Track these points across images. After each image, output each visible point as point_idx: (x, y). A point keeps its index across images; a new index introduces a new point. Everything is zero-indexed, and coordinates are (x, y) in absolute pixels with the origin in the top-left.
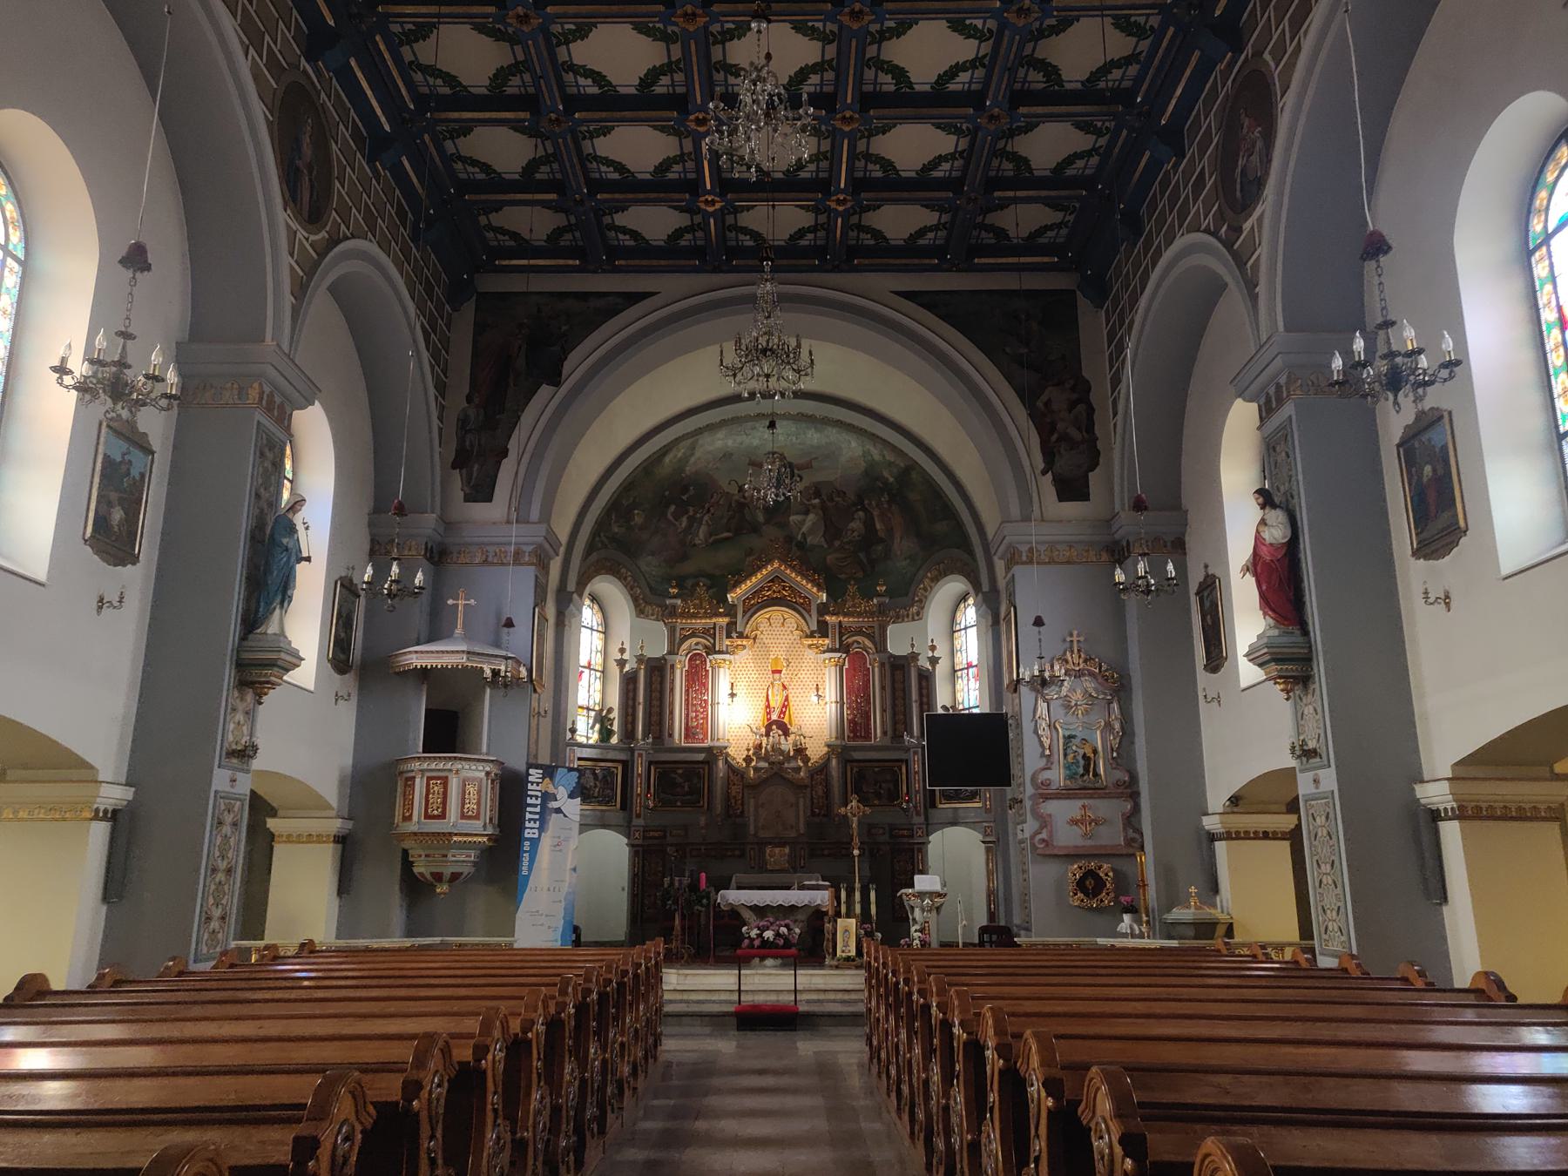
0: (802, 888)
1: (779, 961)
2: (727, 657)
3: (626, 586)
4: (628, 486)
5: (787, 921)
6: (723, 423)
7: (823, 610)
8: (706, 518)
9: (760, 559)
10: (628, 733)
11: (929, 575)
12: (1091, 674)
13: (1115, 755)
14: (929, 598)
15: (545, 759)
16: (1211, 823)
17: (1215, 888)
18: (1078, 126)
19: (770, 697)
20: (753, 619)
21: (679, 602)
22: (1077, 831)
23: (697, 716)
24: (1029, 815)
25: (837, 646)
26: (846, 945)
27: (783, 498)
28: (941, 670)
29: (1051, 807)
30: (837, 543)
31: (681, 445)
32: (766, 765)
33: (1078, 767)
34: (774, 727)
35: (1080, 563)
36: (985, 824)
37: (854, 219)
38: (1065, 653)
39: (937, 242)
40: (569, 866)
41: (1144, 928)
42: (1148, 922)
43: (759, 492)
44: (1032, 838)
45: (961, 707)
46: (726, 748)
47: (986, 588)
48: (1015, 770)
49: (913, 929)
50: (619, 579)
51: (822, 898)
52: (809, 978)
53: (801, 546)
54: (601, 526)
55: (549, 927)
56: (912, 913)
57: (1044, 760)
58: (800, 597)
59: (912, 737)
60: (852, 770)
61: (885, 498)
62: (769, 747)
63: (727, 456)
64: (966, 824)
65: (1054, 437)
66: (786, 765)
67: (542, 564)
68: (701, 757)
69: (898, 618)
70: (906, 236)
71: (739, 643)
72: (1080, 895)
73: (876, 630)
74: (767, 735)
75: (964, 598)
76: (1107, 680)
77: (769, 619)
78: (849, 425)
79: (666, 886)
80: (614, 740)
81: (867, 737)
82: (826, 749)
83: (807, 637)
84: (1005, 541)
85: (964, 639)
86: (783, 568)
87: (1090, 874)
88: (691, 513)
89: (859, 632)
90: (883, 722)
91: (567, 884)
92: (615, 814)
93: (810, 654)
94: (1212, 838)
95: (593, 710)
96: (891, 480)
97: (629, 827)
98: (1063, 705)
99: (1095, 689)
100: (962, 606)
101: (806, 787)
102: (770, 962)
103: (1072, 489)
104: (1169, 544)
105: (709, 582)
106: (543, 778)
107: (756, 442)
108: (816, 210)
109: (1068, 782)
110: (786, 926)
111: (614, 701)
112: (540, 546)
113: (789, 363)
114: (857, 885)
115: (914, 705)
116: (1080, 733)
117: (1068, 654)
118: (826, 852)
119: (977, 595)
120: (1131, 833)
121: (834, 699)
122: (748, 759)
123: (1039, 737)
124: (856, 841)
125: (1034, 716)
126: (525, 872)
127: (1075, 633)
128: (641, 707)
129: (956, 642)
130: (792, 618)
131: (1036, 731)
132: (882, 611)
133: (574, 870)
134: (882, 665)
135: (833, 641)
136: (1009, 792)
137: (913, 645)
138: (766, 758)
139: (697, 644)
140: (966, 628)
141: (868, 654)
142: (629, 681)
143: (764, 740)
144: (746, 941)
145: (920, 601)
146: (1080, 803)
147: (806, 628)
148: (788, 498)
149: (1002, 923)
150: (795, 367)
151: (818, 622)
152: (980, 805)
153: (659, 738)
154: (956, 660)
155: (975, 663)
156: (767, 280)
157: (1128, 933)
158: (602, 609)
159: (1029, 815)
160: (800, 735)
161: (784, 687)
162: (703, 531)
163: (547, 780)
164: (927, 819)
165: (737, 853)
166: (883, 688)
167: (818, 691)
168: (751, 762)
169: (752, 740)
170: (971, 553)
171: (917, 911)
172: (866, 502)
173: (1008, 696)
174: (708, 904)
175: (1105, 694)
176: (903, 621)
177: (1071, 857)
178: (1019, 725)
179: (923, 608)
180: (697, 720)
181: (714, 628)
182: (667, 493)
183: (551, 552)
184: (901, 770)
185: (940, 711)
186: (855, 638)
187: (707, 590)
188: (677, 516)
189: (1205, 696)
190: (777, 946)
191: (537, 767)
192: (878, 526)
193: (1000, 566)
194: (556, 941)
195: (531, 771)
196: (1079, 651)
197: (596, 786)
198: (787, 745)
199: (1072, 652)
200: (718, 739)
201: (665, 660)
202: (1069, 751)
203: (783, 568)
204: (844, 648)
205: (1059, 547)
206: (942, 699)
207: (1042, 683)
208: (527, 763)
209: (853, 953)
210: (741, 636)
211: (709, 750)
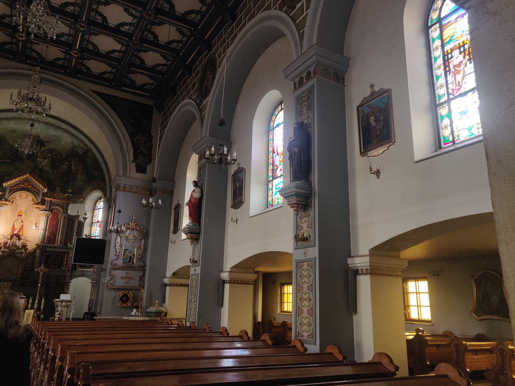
6: (14, 118)
7: (45, 195)
9: (21, 173)
11: (89, 188)
12: (137, 230)
13: (140, 257)
14: (88, 197)
16: (166, 281)
17: (164, 301)
18: (162, 56)
19: (15, 225)
20: (13, 194)
22: (123, 281)
24: (108, 275)
25: (48, 209)
28: (87, 223)
29: (116, 273)
30: (55, 172)
32: (8, 250)
34: (14, 236)
35: (140, 193)
36: (93, 277)
37: (80, 61)
38: (129, 222)
39: (110, 78)
41: (140, 314)
42: (141, 312)
43: (21, 149)
44: (107, 283)
45: (92, 236)
47: (108, 196)
49: (56, 314)
53: (41, 170)
56: (57, 308)
58: (36, 189)
59: (71, 245)
60: (45, 254)
61: (77, 159)
62: (11, 244)
63: (14, 131)
64: (85, 276)
65: (138, 151)
69: (74, 202)
71: (5, 203)
72: (120, 302)
73: (65, 206)
74: (11, 239)
75: (100, 198)
76: (141, 232)
77: (20, 195)
78: (67, 131)
81: (54, 243)
82: (36, 246)
83: (36, 204)
84: (116, 182)
85: (98, 212)
86: (30, 177)
87: (125, 295)
89: (58, 205)
93: (36, 211)
94: (166, 285)
96: (81, 153)
98: (126, 239)
99: (137, 235)
100: (99, 201)
101: (24, 260)
103: (141, 169)
104: (168, 192)
108: (65, 53)
109: (123, 264)
118: (28, 284)
120: (141, 283)
121: (43, 228)
123: (116, 249)
124: (40, 281)
125: (115, 242)
127: (134, 216)
129: (95, 213)
130: (30, 197)
131: (115, 247)
132: (68, 198)
134: (65, 218)
136: (104, 266)
138: (8, 248)
140: (99, 209)
141: (60, 213)
143: (9, 241)
145: (84, 197)
146: (126, 271)
147: (36, 201)
148: (34, 153)
151: (42, 199)
152: (93, 270)
154: (94, 219)
155: (100, 221)
157: (135, 315)
159: (108, 275)
160: (25, 240)
161: (22, 222)
164: (72, 273)
166: (63, 226)
167: (36, 224)
170: (105, 184)
171: (59, 307)
172: (70, 159)
175: (140, 237)
176: (76, 203)
177: (119, 289)
178: (110, 244)
179: (84, 200)
184: (65, 256)
185: (84, 237)
189: (171, 241)
193: (113, 190)
196: (134, 222)
198: (19, 243)
199: (132, 222)
202: (125, 254)
203: (30, 177)
204: (51, 210)
206: (86, 232)
207: (117, 232)
210: (6, 200)
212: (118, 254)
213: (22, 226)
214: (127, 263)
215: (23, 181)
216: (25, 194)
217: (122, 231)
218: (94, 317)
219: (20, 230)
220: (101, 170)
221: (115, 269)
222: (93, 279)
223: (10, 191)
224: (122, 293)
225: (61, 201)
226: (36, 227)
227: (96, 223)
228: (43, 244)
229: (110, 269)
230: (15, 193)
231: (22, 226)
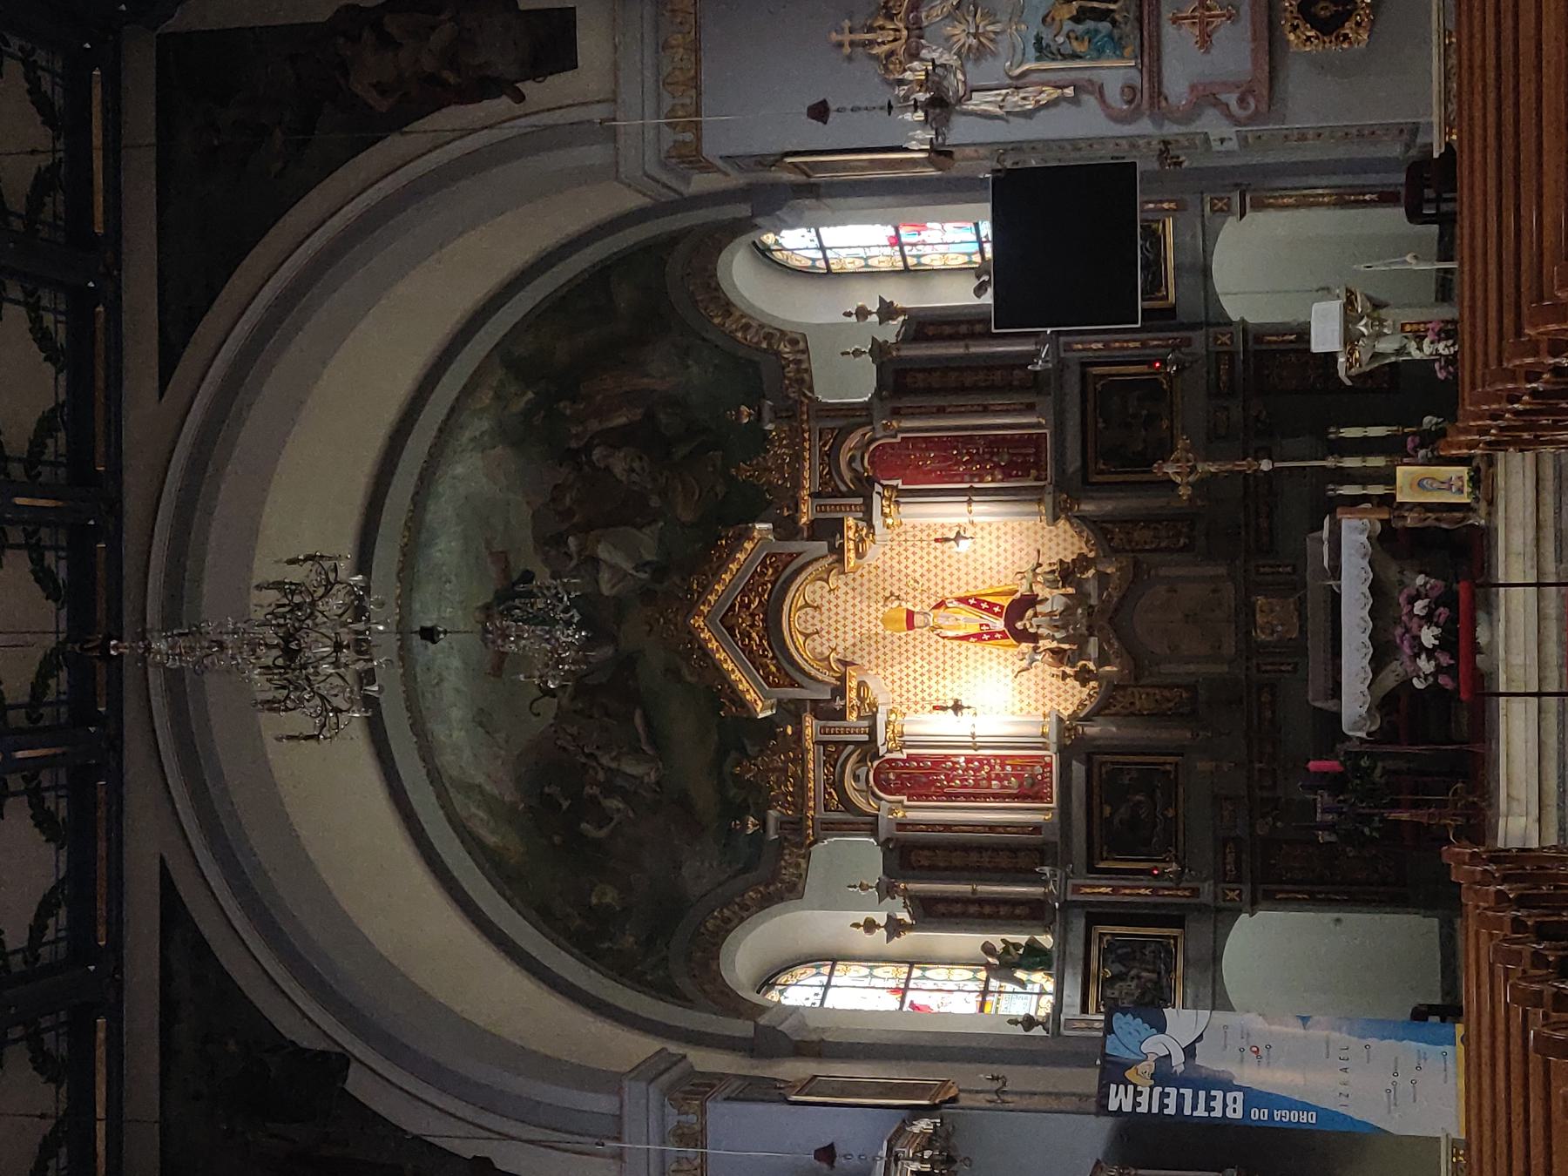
0: (1336, 571)
1: (1481, 616)
3: (742, 920)
4: (544, 916)
5: (1402, 600)
6: (419, 728)
7: (787, 529)
8: (605, 761)
10: (1033, 913)
11: (716, 321)
14: (764, 321)
15: (1087, 1079)
19: (961, 633)
20: (807, 667)
21: (772, 813)
22: (1224, 33)
23: (998, 777)
24: (1192, 128)
25: (860, 501)
26: (1447, 485)
27: (574, 612)
28: (905, 297)
29: (1177, 86)
30: (655, 502)
31: (464, 814)
32: (1093, 641)
33: (1097, 31)
34: (1019, 625)
35: (698, 26)
36: (1208, 208)
39: (62, 307)
40: (1300, 1031)
44: (1237, 122)
45: (977, 258)
46: (1060, 720)
47: (744, 210)
48: (1103, 155)
49: (1416, 355)
50: (729, 931)
51: (1355, 533)
52: (1513, 558)
53: (660, 571)
54: (623, 970)
55: (1418, 1068)
56: (1383, 355)
57: (1085, 97)
58: (763, 574)
59: (1037, 354)
61: (566, 407)
62: (1058, 635)
63: (483, 720)
64: (1207, 253)
66: (1093, 601)
67: (702, 1087)
69: (803, 380)
70: (49, 368)
71: (853, 694)
73: (831, 424)
74: (1035, 638)
75: (763, 252)
77: (807, 636)
78: (421, 478)
79: (1333, 838)
80: (1047, 940)
82: (1061, 523)
83: (841, 560)
85: (843, 253)
86: (705, 609)
88: (596, 790)
89: (831, 457)
90: (1007, 412)
91: (1335, 1035)
92: (1196, 934)
93: (874, 552)
95: (987, 982)
96: (530, 395)
97: (1219, 910)
100: (778, 255)
101: (1136, 564)
102: (1482, 636)
105: (734, 755)
106: (1126, 1083)
107: (456, 663)
109: (1127, 52)
110: (1412, 601)
111: (969, 941)
112: (668, 1092)
113: (313, 604)
114: (1330, 463)
116: (1031, 28)
117: (876, 50)
118: (1264, 524)
119: (756, 227)
121: (964, 508)
122: (1083, 677)
123: (1039, 108)
124: (1243, 465)
126: (1312, 1118)
128: (981, 888)
129: (850, 267)
130: (807, 590)
131: (1028, 115)
132: (789, 413)
133: (1305, 1020)
134: (896, 413)
136: (1146, 164)
137: (857, 353)
138: (1081, 642)
139: (856, 778)
140: (822, 248)
142: (931, 913)
144: (1443, 680)
145: (768, 337)
146: (1168, 30)
147: (825, 563)
149: (1402, 178)
150: (321, 591)
151: (811, 538)
152: (1170, 223)
153: (1042, 853)
154: (885, 267)
155: (890, 231)
156: (148, 649)
158: (788, 966)
159: (1192, 128)
160: (1035, 575)
162: (631, 768)
163: (1129, 1074)
164: (1194, 326)
165: (1265, 698)
166: (941, 411)
167: (947, 540)
168: (1090, 671)
169: (1044, 669)
170: (673, 240)
171: (1385, 346)
172: (574, 445)
173: (959, 168)
174: (1370, 755)
176: (808, 371)
178: (1017, 147)
179: (782, 333)
180: (1007, 777)
181: (825, 744)
182: (557, 839)
183: (675, 1072)
185: (988, 298)
187: (749, 758)
188: (603, 819)
190: (1453, 620)
191: (1103, 1096)
193: (701, 183)
194: (1444, 1054)
195: (1113, 1106)
197: (1139, 977)
198: (1054, 599)
201: (888, 840)
202: (1066, 50)
203: (705, 609)
204: (863, 489)
205: (666, 70)
206: (961, 295)
208: (1097, 1114)
209: (1463, 471)
210: (840, 691)
211: (1062, 750)
212: (1069, 92)
213: (963, 600)
214: (1116, 33)
215: (733, 636)
217: (934, 80)
218: (1436, 155)
219: (984, 606)
220: (602, 274)
221: (1160, 93)
222: (1221, 210)
223: (793, 684)
224: (1295, 28)
225: (807, 445)
226: (958, 537)
227: (907, 249)
228: (1051, 488)
229: (1158, 120)
231: (963, 600)
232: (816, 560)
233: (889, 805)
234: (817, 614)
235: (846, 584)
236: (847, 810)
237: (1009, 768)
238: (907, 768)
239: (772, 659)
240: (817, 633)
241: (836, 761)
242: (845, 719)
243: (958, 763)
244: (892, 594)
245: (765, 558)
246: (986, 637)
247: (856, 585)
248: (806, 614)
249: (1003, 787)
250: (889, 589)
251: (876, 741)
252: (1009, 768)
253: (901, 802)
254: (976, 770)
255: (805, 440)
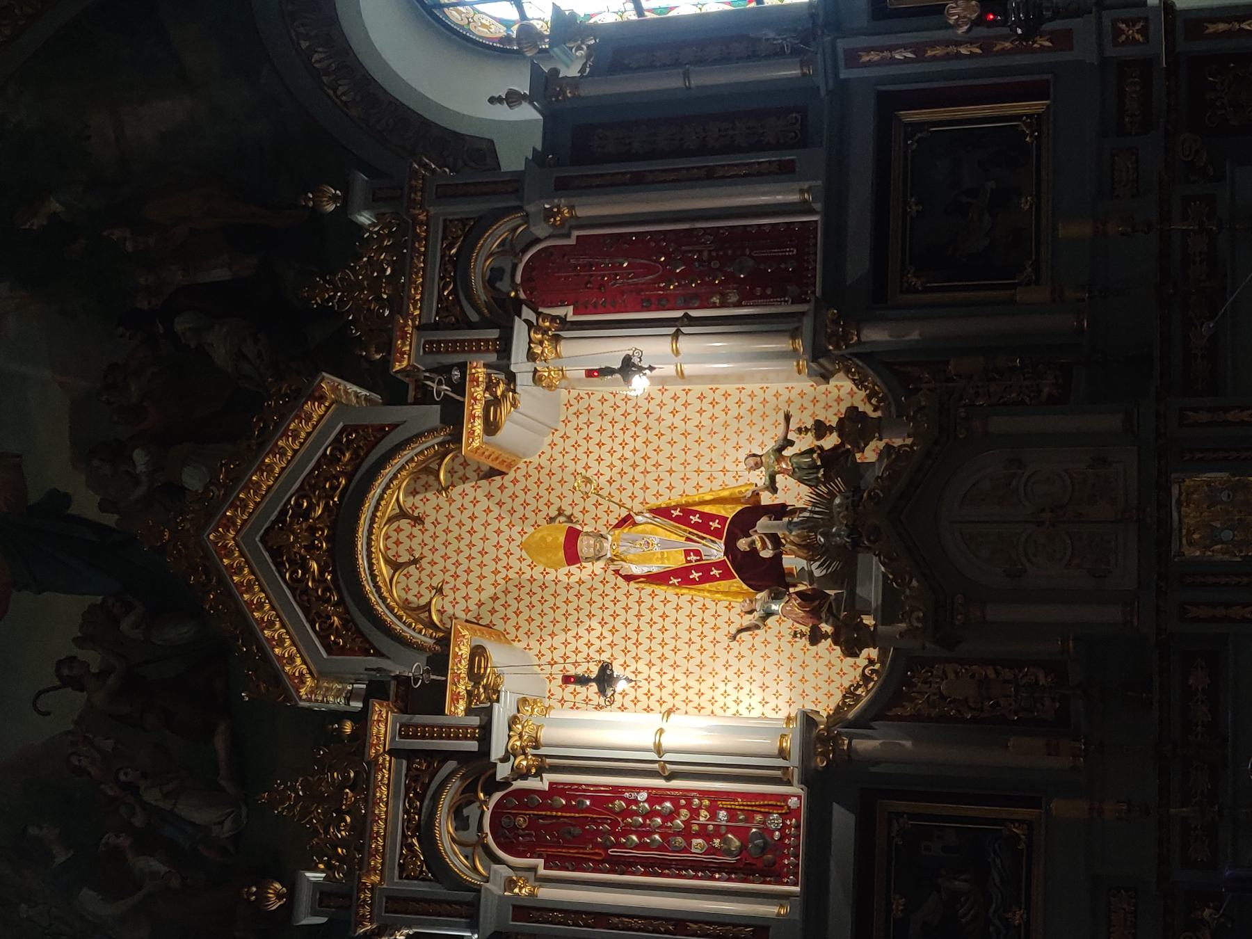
2: (501, 713)
20: (389, 618)
23: (703, 833)
25: (494, 334)
58: (333, 460)
68: (843, 820)
83: (457, 438)
89: (457, 268)
115: (696, 81)
134: (564, 186)
135: (477, 347)
139: (461, 823)
147: (433, 441)
180: (717, 833)
181: (410, 755)
186: (477, 283)
192: (220, 274)
200: (783, 754)
210: (439, 660)
216: (381, 531)
230: (381, 608)
231: (662, 512)
232: (419, 435)
233: (510, 873)
234: (416, 531)
235: (489, 496)
236: (436, 879)
237: (722, 815)
238: (551, 808)
239: (336, 605)
240: (415, 562)
241: (426, 787)
242: (442, 712)
243: (636, 802)
244: (560, 512)
245: (341, 433)
246: (695, 575)
247: (505, 497)
248: (399, 530)
249: (711, 850)
250: (557, 503)
251: (488, 754)
252: (722, 815)
253: (533, 869)
254: (670, 816)
255: (417, 237)
